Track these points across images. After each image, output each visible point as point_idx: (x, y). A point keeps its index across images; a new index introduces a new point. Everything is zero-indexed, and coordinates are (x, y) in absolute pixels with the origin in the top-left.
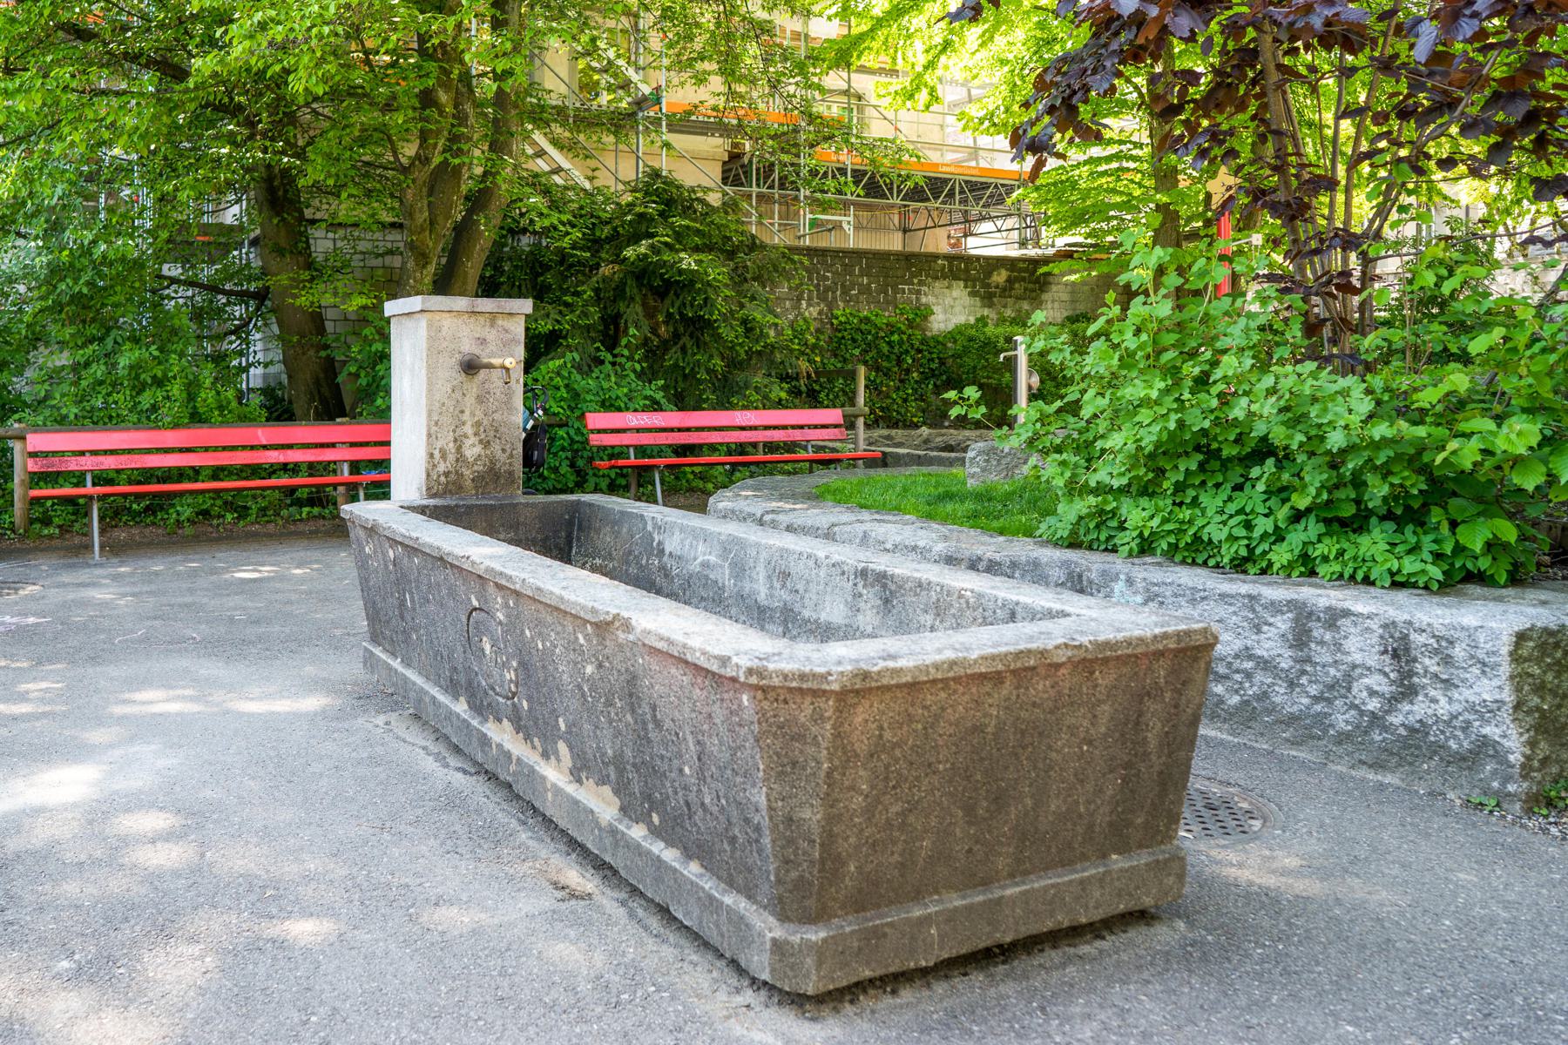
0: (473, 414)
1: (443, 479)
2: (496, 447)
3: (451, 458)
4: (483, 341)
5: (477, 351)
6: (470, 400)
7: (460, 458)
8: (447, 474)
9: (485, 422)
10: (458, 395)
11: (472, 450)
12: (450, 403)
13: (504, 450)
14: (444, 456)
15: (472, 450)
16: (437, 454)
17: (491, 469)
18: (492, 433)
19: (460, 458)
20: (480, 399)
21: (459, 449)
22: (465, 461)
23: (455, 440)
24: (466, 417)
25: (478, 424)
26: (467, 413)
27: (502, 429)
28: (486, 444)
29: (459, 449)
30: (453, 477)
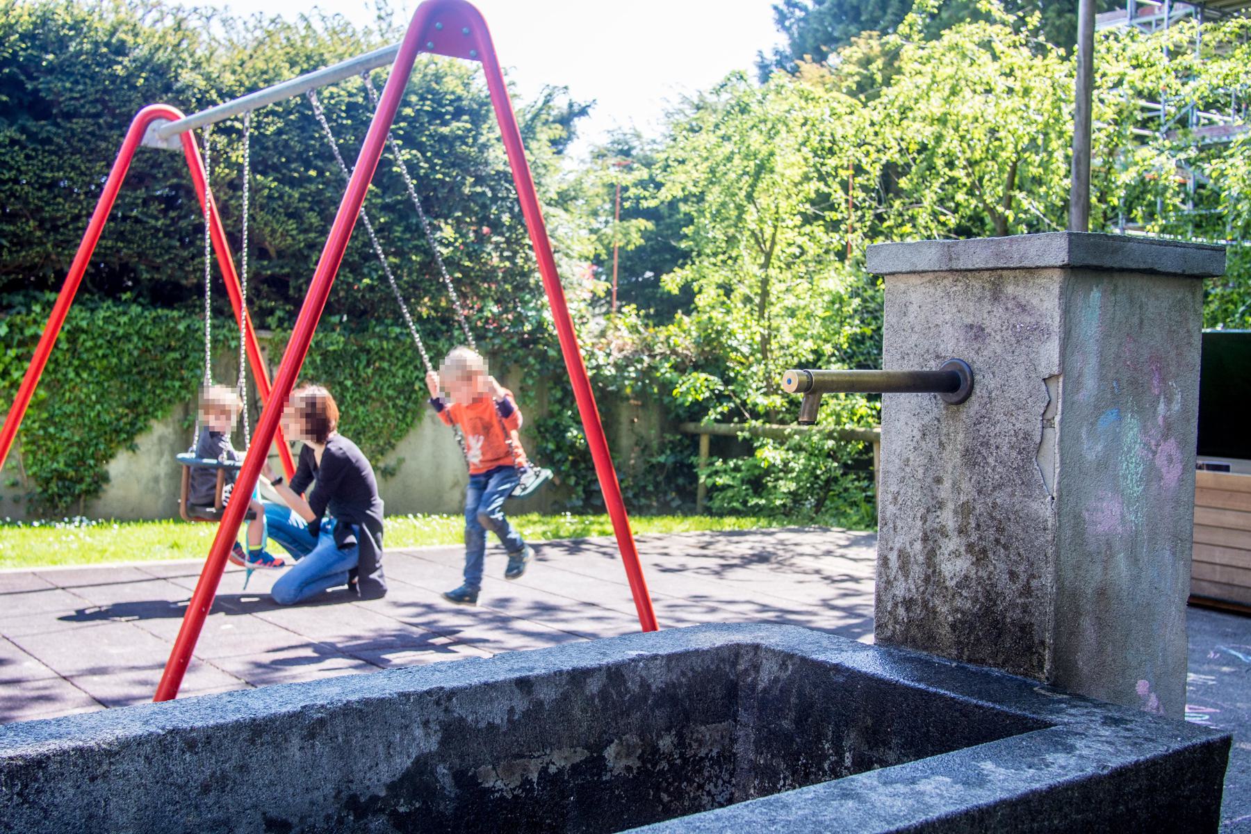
0: (956, 487)
1: (901, 611)
2: (998, 566)
3: (917, 571)
4: (977, 333)
5: (968, 355)
6: (952, 459)
7: (932, 577)
8: (909, 603)
9: (979, 508)
10: (930, 445)
11: (954, 566)
12: (917, 461)
13: (1013, 575)
14: (904, 567)
15: (954, 566)
16: (893, 557)
17: (987, 611)
18: (991, 534)
19: (932, 577)
20: (971, 458)
21: (931, 555)
22: (941, 584)
23: (925, 539)
24: (945, 491)
25: (965, 510)
26: (947, 484)
27: (1012, 528)
28: (980, 556)
29: (931, 555)
30: (918, 611)
